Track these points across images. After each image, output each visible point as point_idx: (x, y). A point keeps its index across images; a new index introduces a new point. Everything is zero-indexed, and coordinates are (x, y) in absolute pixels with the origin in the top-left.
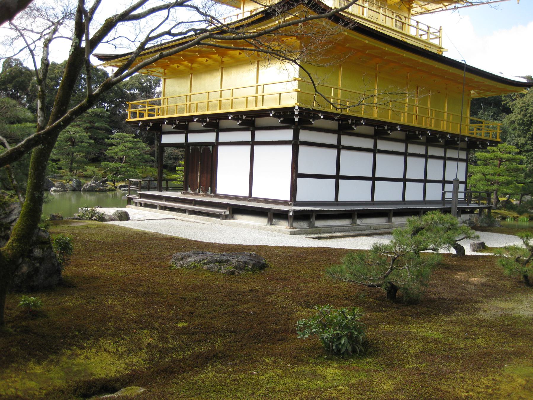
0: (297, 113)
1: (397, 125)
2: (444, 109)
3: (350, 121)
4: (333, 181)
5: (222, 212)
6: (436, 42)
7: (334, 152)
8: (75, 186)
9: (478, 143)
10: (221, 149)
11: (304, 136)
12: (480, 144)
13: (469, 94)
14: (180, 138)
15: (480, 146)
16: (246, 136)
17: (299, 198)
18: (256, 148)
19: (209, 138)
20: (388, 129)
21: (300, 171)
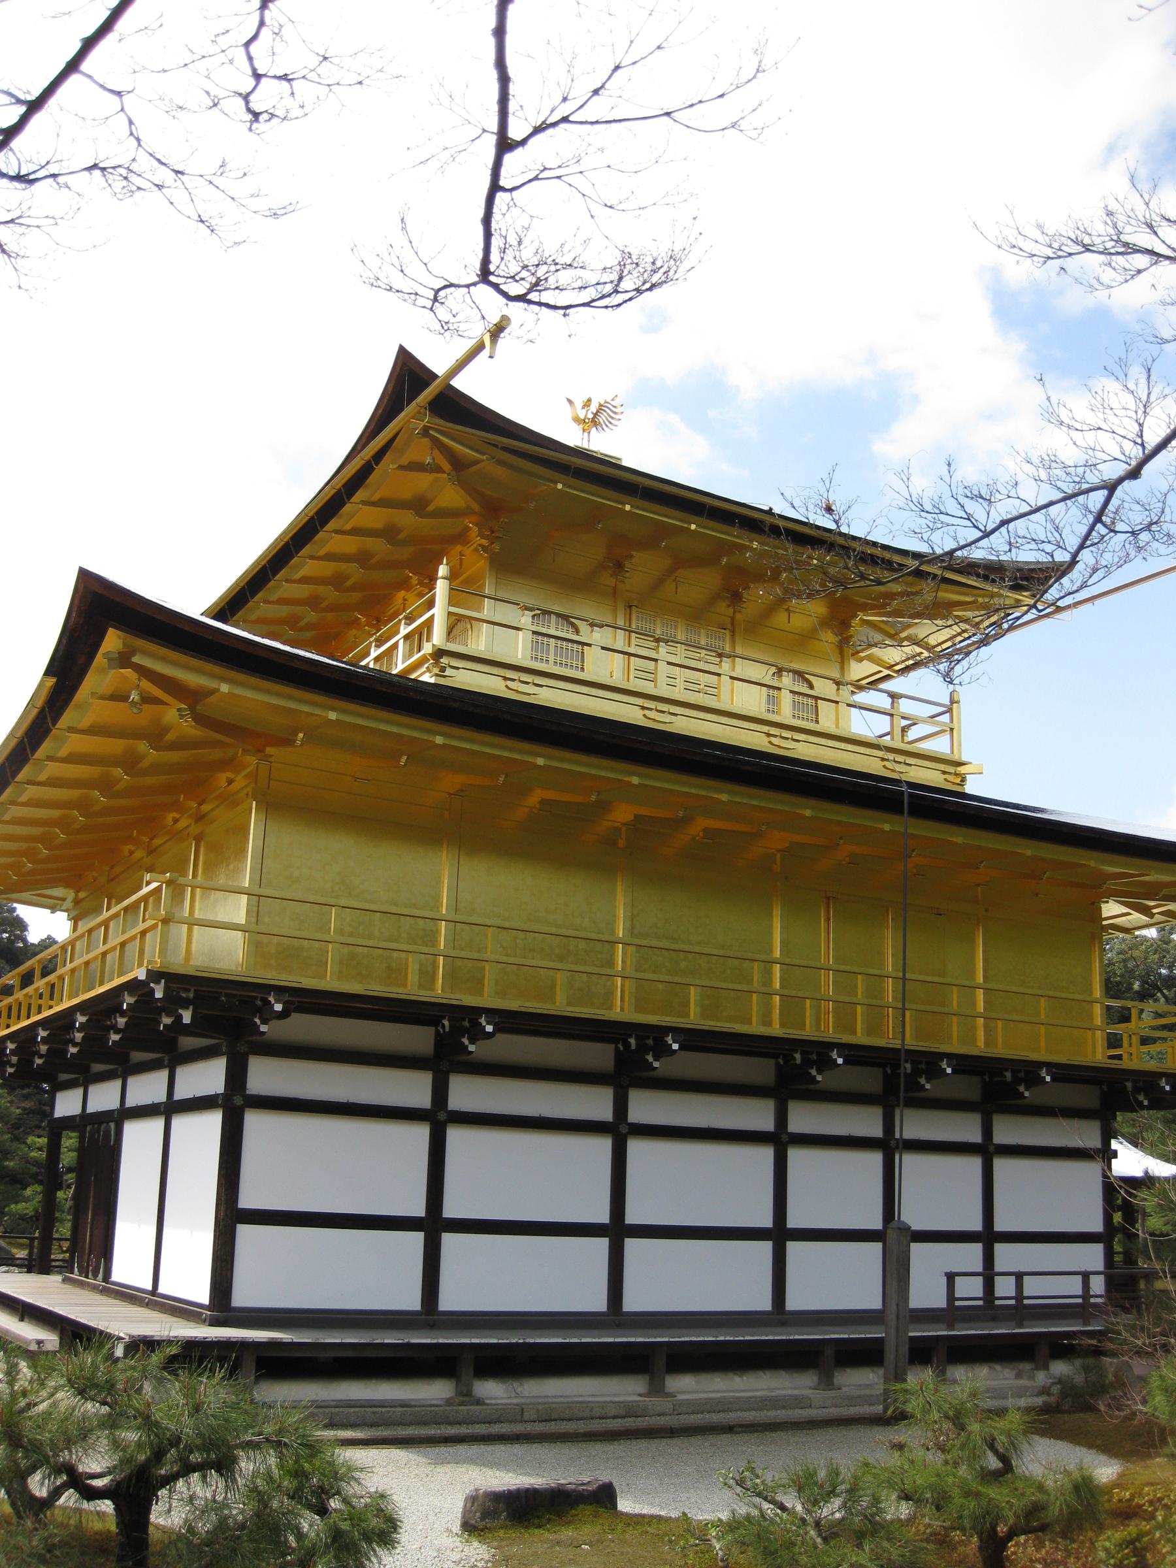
0: (159, 995)
1: (667, 1030)
2: (972, 973)
3: (446, 1022)
4: (450, 1242)
5: (29, 1342)
6: (940, 746)
7: (421, 1133)
9: (1129, 1085)
11: (264, 1076)
12: (1137, 1090)
13: (1095, 915)
15: (1141, 1098)
17: (243, 1296)
20: (643, 1048)
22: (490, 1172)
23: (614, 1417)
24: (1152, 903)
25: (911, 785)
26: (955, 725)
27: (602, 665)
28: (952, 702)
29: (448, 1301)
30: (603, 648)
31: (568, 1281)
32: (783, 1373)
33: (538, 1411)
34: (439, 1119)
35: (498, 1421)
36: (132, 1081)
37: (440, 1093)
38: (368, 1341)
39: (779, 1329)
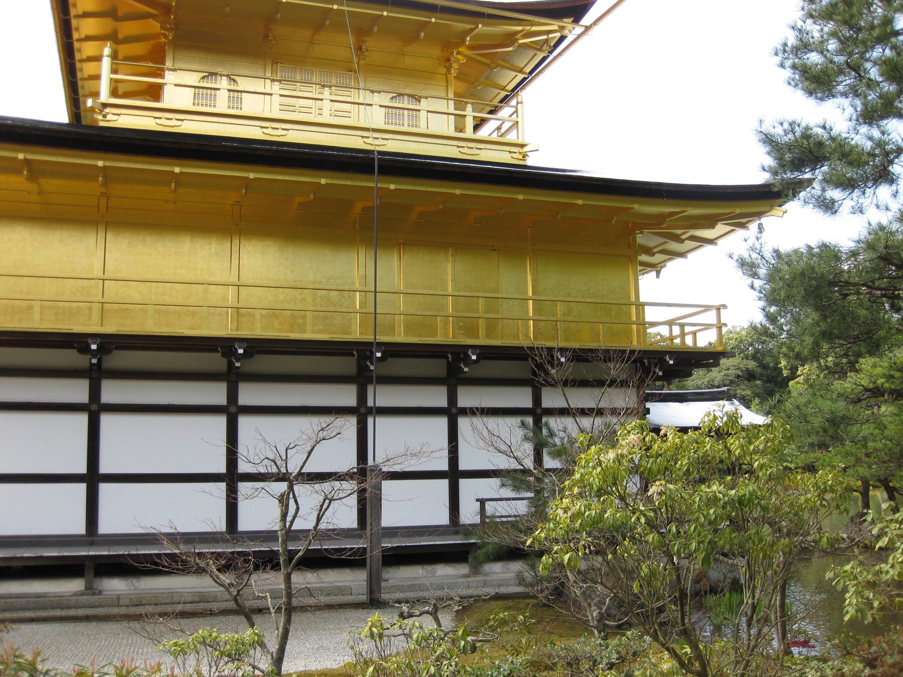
22: (129, 442)
23: (190, 603)
24: (679, 232)
25: (380, 153)
26: (519, 120)
27: (251, 105)
28: (518, 103)
29: (105, 527)
30: (176, 85)
31: (201, 510)
32: (348, 571)
33: (131, 599)
34: (94, 410)
35: (100, 606)
37: (95, 393)
38: (11, 555)
39: (452, 537)
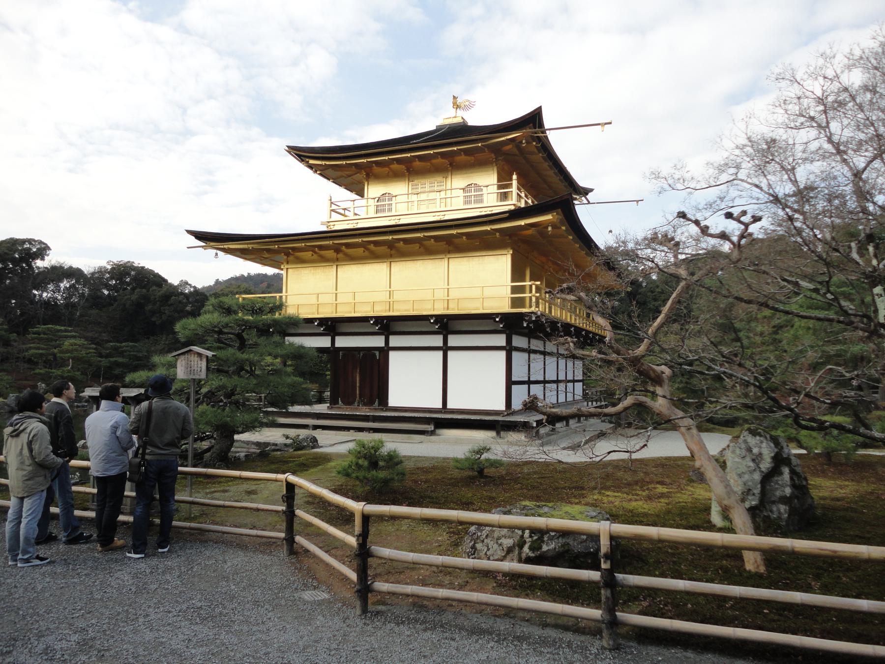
8: (13, 405)
10: (392, 354)
14: (324, 342)
16: (438, 341)
18: (450, 354)
19: (377, 342)
21: (514, 379)
36: (391, 338)
